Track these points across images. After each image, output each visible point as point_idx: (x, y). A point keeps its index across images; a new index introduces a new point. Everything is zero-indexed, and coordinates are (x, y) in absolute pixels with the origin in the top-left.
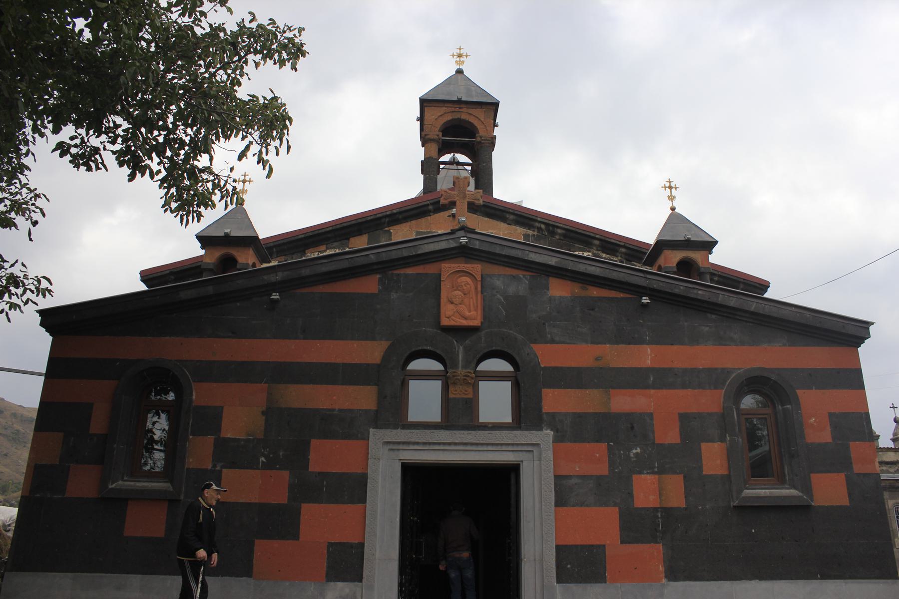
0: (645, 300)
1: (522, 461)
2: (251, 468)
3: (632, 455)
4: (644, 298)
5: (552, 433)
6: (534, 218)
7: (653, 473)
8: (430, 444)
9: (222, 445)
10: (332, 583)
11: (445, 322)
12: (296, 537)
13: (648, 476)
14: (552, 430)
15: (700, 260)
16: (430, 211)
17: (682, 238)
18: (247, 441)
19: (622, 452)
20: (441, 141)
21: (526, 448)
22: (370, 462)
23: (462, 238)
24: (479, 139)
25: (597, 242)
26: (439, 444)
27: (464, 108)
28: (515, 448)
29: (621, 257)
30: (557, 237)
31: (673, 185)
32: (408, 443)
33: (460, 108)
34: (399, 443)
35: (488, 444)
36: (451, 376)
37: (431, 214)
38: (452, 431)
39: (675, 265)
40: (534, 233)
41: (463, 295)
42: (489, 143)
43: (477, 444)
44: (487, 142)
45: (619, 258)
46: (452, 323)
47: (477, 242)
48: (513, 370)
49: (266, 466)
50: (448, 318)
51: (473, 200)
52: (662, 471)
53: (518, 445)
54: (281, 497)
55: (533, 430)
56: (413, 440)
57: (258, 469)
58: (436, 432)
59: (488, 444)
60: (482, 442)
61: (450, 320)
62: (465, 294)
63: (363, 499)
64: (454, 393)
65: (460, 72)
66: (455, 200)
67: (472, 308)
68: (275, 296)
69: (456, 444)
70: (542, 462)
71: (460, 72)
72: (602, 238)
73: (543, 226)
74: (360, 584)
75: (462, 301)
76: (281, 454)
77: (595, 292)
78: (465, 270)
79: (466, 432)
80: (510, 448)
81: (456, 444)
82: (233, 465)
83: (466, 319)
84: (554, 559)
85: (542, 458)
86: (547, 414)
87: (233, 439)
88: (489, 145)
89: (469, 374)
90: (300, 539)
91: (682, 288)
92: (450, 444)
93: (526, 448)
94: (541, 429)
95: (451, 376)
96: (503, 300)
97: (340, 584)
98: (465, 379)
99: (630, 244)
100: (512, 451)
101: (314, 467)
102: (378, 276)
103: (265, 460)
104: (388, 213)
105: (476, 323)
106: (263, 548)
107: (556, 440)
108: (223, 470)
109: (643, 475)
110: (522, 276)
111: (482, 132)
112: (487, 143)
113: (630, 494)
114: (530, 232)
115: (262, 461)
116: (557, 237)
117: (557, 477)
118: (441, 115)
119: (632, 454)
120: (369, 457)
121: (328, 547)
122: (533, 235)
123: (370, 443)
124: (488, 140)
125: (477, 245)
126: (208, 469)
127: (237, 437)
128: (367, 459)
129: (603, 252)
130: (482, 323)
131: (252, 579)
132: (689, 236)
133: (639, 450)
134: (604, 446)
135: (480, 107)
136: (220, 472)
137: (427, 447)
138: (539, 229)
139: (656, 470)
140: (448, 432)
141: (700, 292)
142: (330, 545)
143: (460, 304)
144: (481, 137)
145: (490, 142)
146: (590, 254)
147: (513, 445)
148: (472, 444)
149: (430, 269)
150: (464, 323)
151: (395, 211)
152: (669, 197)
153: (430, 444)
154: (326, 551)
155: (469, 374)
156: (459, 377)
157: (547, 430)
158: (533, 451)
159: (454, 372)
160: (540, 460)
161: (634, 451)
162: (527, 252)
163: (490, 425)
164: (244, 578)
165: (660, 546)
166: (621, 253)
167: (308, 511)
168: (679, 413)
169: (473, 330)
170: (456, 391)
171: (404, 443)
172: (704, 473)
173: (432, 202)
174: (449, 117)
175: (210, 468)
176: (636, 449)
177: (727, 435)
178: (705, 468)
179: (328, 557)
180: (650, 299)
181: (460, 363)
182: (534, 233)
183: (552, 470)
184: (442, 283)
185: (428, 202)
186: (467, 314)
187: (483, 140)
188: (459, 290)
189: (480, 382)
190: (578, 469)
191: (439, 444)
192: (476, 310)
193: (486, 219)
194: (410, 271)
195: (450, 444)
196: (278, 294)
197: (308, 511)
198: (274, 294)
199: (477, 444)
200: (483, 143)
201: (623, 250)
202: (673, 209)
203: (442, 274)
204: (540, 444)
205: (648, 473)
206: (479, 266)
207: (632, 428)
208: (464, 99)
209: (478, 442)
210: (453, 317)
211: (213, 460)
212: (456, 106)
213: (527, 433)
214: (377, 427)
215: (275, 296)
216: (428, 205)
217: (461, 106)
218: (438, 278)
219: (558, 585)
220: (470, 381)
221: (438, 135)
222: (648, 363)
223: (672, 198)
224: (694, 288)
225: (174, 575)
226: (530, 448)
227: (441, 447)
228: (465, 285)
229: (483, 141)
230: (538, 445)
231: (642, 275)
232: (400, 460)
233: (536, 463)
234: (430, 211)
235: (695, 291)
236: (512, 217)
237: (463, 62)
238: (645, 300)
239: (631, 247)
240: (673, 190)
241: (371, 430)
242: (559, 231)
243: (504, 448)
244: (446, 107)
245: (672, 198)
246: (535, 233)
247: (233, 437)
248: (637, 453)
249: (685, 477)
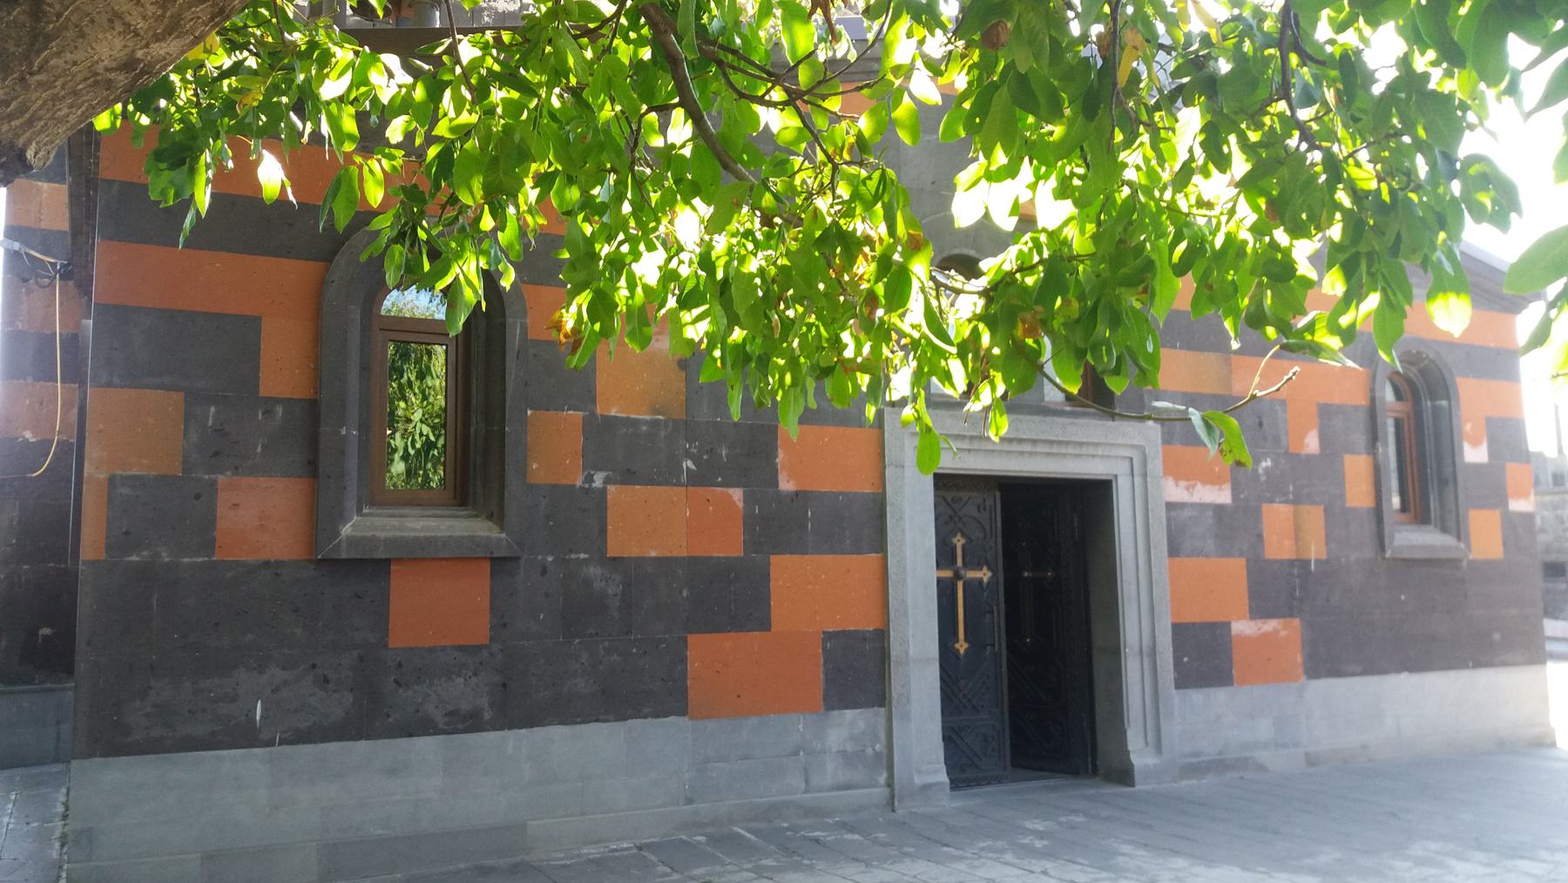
2: (668, 483)
3: (1260, 471)
7: (1287, 502)
9: (601, 434)
10: (836, 713)
12: (765, 625)
18: (654, 424)
49: (697, 480)
52: (1297, 501)
54: (729, 545)
57: (679, 484)
60: (1061, 439)
74: (883, 710)
76: (724, 453)
82: (628, 477)
87: (622, 418)
90: (773, 629)
97: (849, 714)
101: (786, 485)
103: (693, 467)
106: (703, 651)
108: (609, 487)
113: (1260, 536)
115: (687, 468)
121: (824, 641)
126: (574, 485)
127: (633, 416)
131: (686, 718)
136: (603, 491)
139: (1291, 497)
142: (829, 636)
154: (821, 651)
164: (672, 719)
165: (1296, 622)
167: (786, 570)
168: (1318, 404)
175: (579, 483)
178: (1348, 496)
179: (825, 662)
197: (786, 570)
205: (1281, 502)
207: (1261, 424)
211: (584, 468)
225: (521, 727)
247: (624, 415)
248: (1267, 468)
249: (1325, 510)
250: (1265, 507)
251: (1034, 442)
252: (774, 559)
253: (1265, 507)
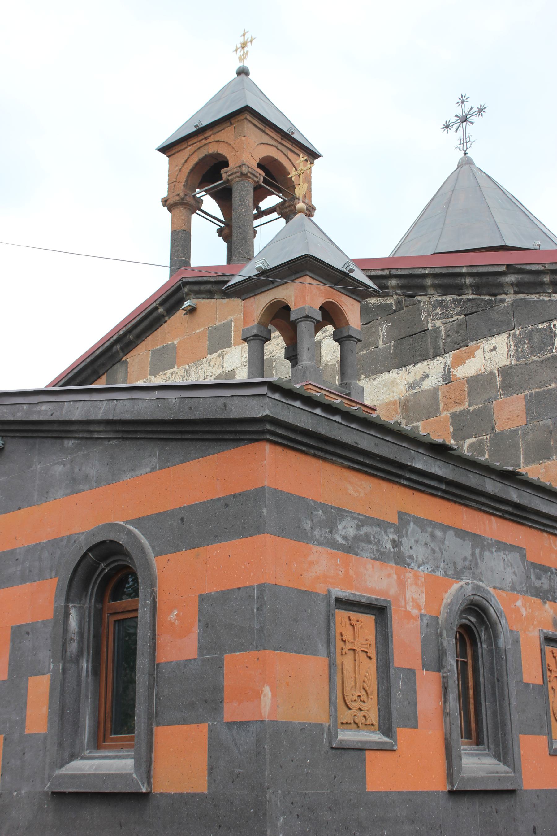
15: (293, 299)
16: (163, 316)
27: (210, 136)
29: (397, 294)
33: (206, 139)
37: (166, 318)
42: (238, 177)
44: (234, 176)
45: (395, 297)
65: (243, 72)
71: (243, 72)
88: (240, 179)
99: (397, 269)
112: (235, 178)
118: (186, 161)
124: (235, 173)
135: (229, 124)
145: (238, 174)
166: (393, 288)
173: (158, 302)
174: (195, 159)
185: (155, 305)
187: (229, 176)
193: (225, 301)
200: (232, 180)
212: (200, 138)
216: (156, 308)
217: (206, 136)
221: (179, 195)
229: (249, 175)
234: (163, 316)
244: (190, 146)
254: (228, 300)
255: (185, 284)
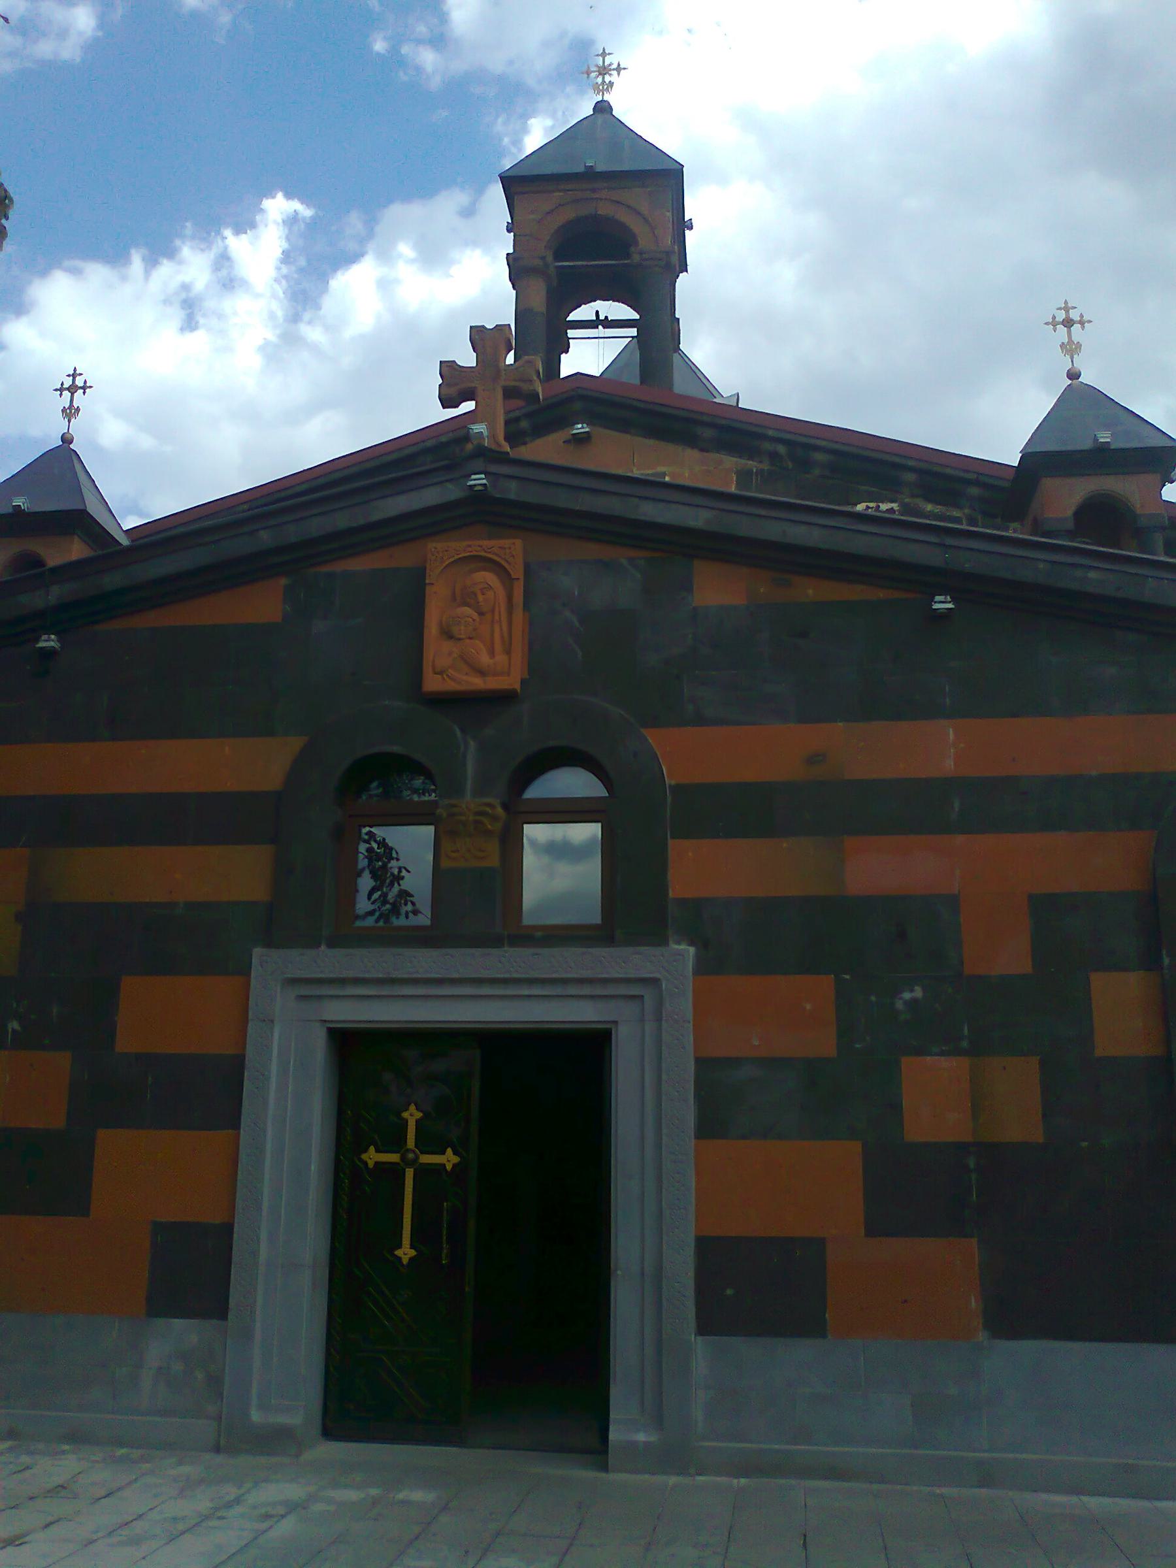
0: (943, 603)
1: (616, 1022)
3: (899, 1005)
4: (938, 598)
5: (692, 950)
6: (759, 430)
7: (958, 1052)
8: (393, 981)
10: (160, 1322)
11: (432, 683)
12: (83, 1209)
13: (945, 1062)
14: (691, 944)
17: (1087, 445)
19: (873, 998)
20: (552, 271)
21: (623, 990)
22: (251, 1029)
23: (473, 477)
24: (636, 258)
25: (910, 477)
26: (415, 982)
28: (599, 991)
30: (817, 472)
31: (1074, 315)
32: (343, 982)
33: (594, 190)
34: (320, 982)
35: (531, 982)
36: (445, 815)
37: (527, 439)
38: (444, 951)
39: (1070, 513)
40: (761, 466)
41: (475, 616)
43: (505, 982)
45: (967, 511)
46: (450, 686)
47: (513, 485)
48: (607, 795)
50: (441, 673)
51: (517, 384)
53: (605, 981)
55: (639, 945)
56: (351, 974)
58: (408, 952)
59: (531, 982)
60: (515, 975)
61: (444, 679)
62: (481, 614)
63: (233, 1121)
64: (454, 855)
66: (473, 385)
67: (498, 647)
68: (49, 642)
69: (453, 982)
70: (664, 1025)
72: (922, 465)
73: (782, 449)
75: (475, 630)
76: (55, 1011)
77: (811, 591)
78: (483, 554)
79: (477, 952)
80: (586, 990)
81: (453, 982)
83: (482, 673)
84: (691, 1274)
85: (664, 1015)
86: (682, 902)
89: (488, 810)
91: (1041, 566)
92: (440, 982)
93: (623, 990)
94: (664, 942)
95: (445, 815)
96: (577, 624)
97: (177, 1323)
98: (476, 822)
100: (592, 997)
101: (126, 1043)
102: (284, 581)
104: (429, 444)
105: (511, 682)
107: (702, 968)
109: (929, 1058)
110: (624, 562)
111: (644, 242)
114: (753, 465)
115: (13, 1029)
116: (817, 472)
117: (704, 1064)
119: (901, 1002)
120: (250, 1017)
122: (760, 472)
123: (253, 982)
125: (512, 490)
128: (246, 1021)
129: (929, 501)
130: (523, 682)
132: (1104, 437)
133: (918, 993)
134: (825, 984)
137: (385, 991)
138: (773, 456)
139: (965, 1044)
140: (435, 953)
141: (1092, 575)
143: (470, 638)
144: (641, 253)
145: (662, 263)
146: (895, 506)
147: (590, 981)
148: (493, 981)
149: (401, 558)
150: (477, 683)
151: (444, 439)
152: (1062, 345)
153: (393, 981)
155: (488, 810)
156: (463, 818)
157: (679, 943)
158: (643, 996)
159: (454, 806)
160: (659, 1020)
161: (907, 996)
162: (636, 500)
163: (539, 934)
169: (503, 698)
170: (458, 851)
171: (331, 982)
172: (1099, 1052)
174: (569, 214)
176: (912, 991)
177: (1164, 952)
180: (953, 600)
181: (469, 783)
182: (761, 466)
183: (690, 1048)
184: (429, 590)
186: (485, 659)
188: (468, 605)
189: (525, 826)
190: (756, 1043)
191: (415, 982)
192: (508, 652)
193: (651, 442)
194: (357, 565)
195: (440, 982)
196: (53, 637)
198: (44, 637)
199: (505, 982)
201: (974, 491)
202: (1073, 375)
203: (428, 566)
204: (659, 979)
205: (942, 1054)
206: (519, 543)
208: (599, 169)
209: (507, 976)
210: (451, 671)
213: (627, 951)
214: (269, 945)
215: (49, 642)
218: (417, 580)
219: (699, 1338)
220: (489, 827)
221: (543, 258)
222: (949, 766)
223: (1071, 348)
224: (1073, 565)
226: (635, 990)
227: (421, 991)
228: (481, 590)
230: (655, 982)
231: (933, 539)
232: (325, 1021)
233: (649, 1027)
235: (1079, 573)
236: (708, 433)
237: (611, 84)
238: (943, 603)
239: (991, 481)
240: (1076, 328)
241: (257, 952)
242: (819, 457)
243: (572, 990)
245: (1071, 348)
246: (766, 466)
248: (915, 1001)
250: (907, 1062)
251: (479, 981)
252: (102, 1134)
253: (907, 1062)
254: (657, 442)
255: (583, 398)
